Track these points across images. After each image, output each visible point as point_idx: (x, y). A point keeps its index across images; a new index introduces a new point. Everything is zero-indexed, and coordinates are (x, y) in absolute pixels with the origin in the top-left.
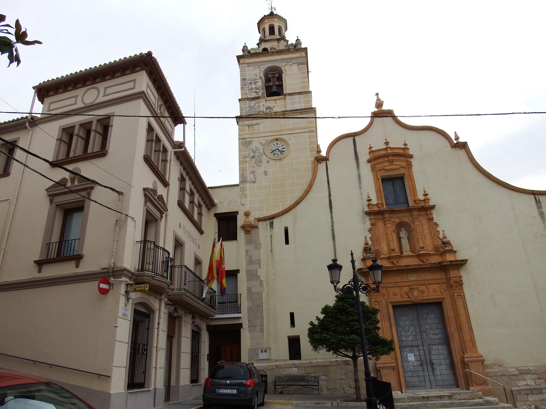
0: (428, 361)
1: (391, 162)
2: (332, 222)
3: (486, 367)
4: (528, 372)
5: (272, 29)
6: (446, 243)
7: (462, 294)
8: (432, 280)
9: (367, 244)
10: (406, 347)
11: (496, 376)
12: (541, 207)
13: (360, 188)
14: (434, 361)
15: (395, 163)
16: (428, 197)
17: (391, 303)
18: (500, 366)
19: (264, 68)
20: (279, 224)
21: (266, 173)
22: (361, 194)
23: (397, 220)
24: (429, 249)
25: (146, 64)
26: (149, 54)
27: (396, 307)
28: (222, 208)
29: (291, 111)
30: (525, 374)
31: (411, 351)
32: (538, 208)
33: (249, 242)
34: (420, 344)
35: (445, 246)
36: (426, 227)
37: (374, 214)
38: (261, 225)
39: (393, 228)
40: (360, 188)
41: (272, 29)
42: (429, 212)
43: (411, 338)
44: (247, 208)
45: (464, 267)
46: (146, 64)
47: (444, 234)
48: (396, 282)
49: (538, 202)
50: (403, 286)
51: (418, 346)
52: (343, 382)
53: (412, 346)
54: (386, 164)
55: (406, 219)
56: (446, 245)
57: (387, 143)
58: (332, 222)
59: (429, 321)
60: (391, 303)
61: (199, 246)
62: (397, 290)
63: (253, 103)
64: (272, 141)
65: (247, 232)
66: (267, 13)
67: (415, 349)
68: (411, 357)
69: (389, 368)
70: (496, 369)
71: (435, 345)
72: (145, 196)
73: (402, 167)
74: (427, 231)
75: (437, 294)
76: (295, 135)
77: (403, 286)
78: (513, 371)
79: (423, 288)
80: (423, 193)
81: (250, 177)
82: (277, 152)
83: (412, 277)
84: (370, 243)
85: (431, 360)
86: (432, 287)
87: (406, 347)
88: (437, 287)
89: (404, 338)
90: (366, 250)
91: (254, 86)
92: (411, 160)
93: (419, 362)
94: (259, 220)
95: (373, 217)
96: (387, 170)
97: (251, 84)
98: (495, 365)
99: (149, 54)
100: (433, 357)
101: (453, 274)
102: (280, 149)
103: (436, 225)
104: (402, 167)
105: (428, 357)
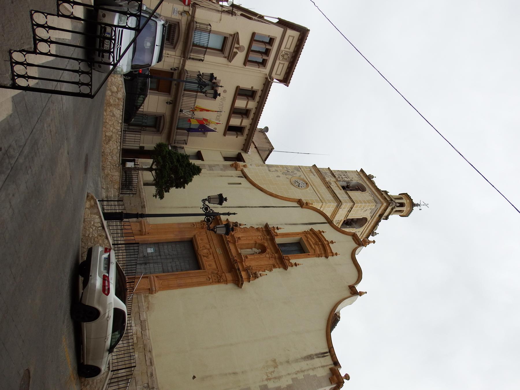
0: (148, 261)
1: (316, 244)
2: (252, 207)
3: (146, 297)
4: (143, 328)
5: (402, 205)
6: (256, 276)
7: (211, 281)
8: (220, 263)
9: (240, 225)
10: (159, 248)
11: (138, 302)
12: (319, 357)
13: (286, 224)
14: (148, 265)
15: (317, 247)
16: (294, 267)
17: (195, 236)
18: (148, 308)
19: (360, 182)
20: (243, 180)
21: (278, 176)
22: (281, 224)
23: (266, 245)
24: (247, 264)
25: (303, 33)
26: (308, 30)
27: (191, 243)
28: (244, 155)
29: (333, 190)
30: (141, 326)
31: (155, 251)
32: (316, 355)
33: (224, 165)
34: (162, 257)
35: (253, 275)
36: (267, 263)
37: (268, 231)
38: (239, 173)
39: (259, 242)
40: (286, 224)
41: (402, 205)
42: (280, 265)
43: (166, 251)
44: (248, 165)
45: (236, 287)
46: (303, 33)
47: (264, 275)
48: (212, 240)
49: (323, 355)
50: (210, 245)
51: (160, 256)
52: (129, 204)
53: (160, 252)
54: (313, 240)
55: (268, 250)
56: (254, 275)
57: (332, 242)
58: (252, 207)
59: (182, 264)
60: (195, 236)
61: (215, 110)
62: (206, 241)
63: (330, 174)
64: (305, 181)
65: (232, 165)
66: (415, 202)
67: (157, 254)
68: (150, 250)
69: (141, 227)
70: (145, 305)
71: (162, 266)
72: (234, 34)
73: (314, 250)
74: (262, 263)
75: (208, 267)
76: (314, 193)
77: (210, 245)
78: (144, 316)
79: (211, 257)
80: (297, 263)
81: (273, 169)
82: (297, 184)
83: (219, 251)
84: (242, 227)
85: (149, 263)
86: (214, 264)
87: (159, 248)
88: (214, 266)
89: (166, 247)
90: (236, 224)
91: (344, 177)
92: (323, 258)
93: (146, 255)
94: (242, 171)
95: (264, 229)
96: (308, 241)
97: (344, 175)
98: (148, 303)
99: (308, 30)
100: (152, 265)
101: (229, 276)
102: (300, 185)
103: (271, 270)
104: (314, 250)
105: (152, 261)
